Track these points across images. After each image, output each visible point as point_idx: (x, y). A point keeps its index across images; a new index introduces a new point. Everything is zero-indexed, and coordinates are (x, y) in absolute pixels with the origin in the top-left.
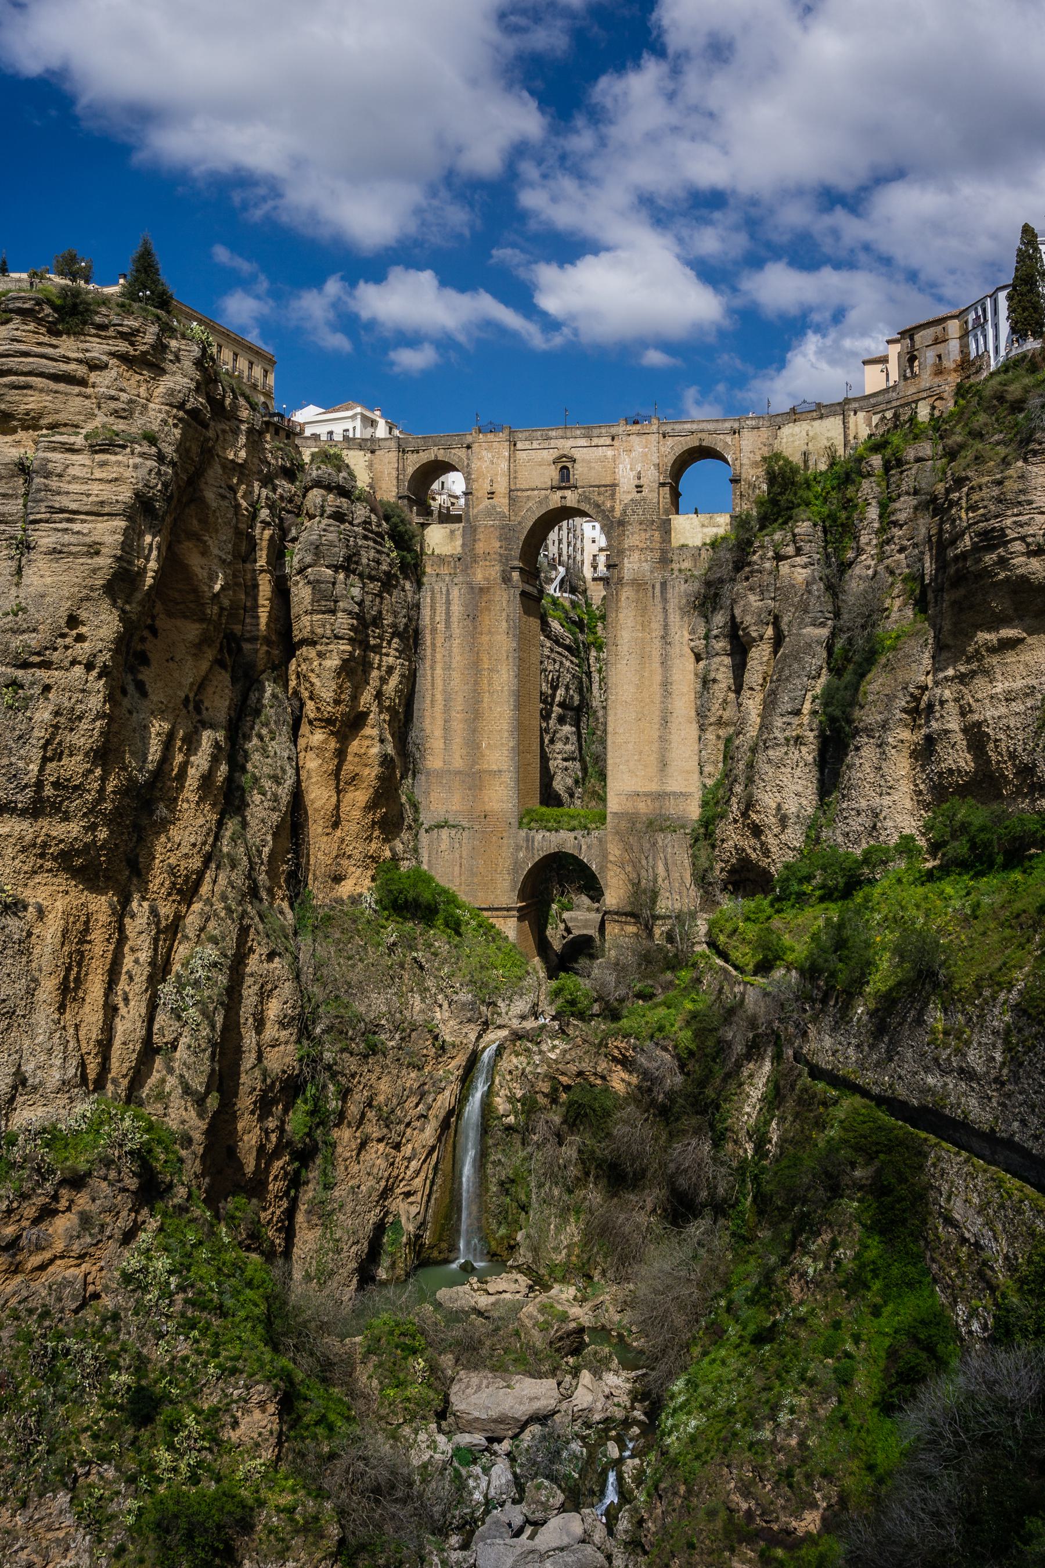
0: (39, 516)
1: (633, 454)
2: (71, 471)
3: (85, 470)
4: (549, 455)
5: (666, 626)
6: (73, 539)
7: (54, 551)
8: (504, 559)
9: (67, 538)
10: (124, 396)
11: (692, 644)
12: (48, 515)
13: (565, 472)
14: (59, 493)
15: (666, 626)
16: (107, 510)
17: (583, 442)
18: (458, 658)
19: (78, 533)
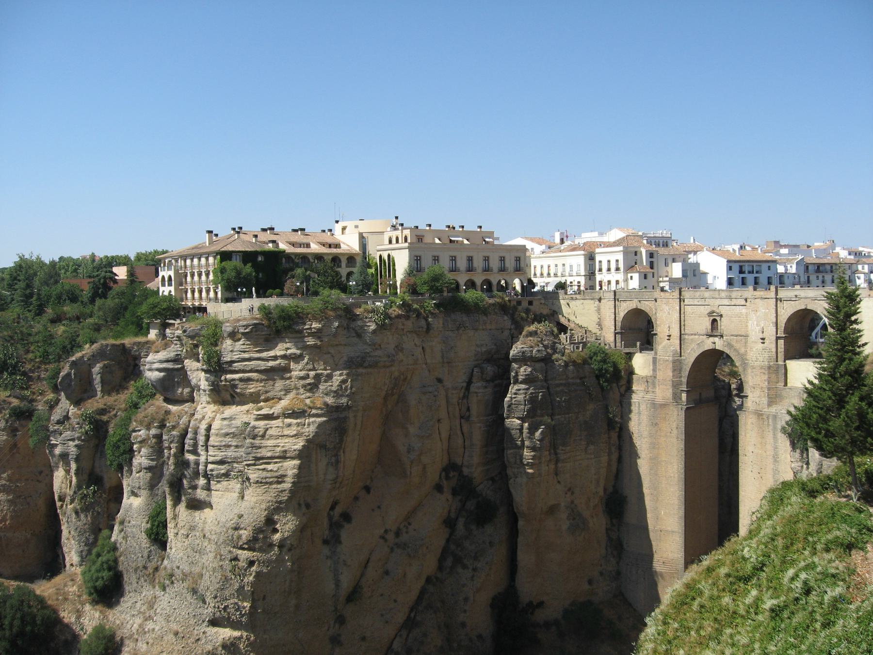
0: (249, 462)
1: (758, 313)
2: (269, 432)
3: (279, 429)
4: (706, 310)
5: (776, 448)
6: (269, 475)
7: (257, 482)
8: (676, 385)
9: (265, 474)
10: (312, 374)
11: (793, 465)
12: (253, 462)
13: (714, 321)
14: (260, 447)
15: (776, 448)
16: (288, 455)
17: (726, 302)
18: (646, 452)
19: (271, 471)
